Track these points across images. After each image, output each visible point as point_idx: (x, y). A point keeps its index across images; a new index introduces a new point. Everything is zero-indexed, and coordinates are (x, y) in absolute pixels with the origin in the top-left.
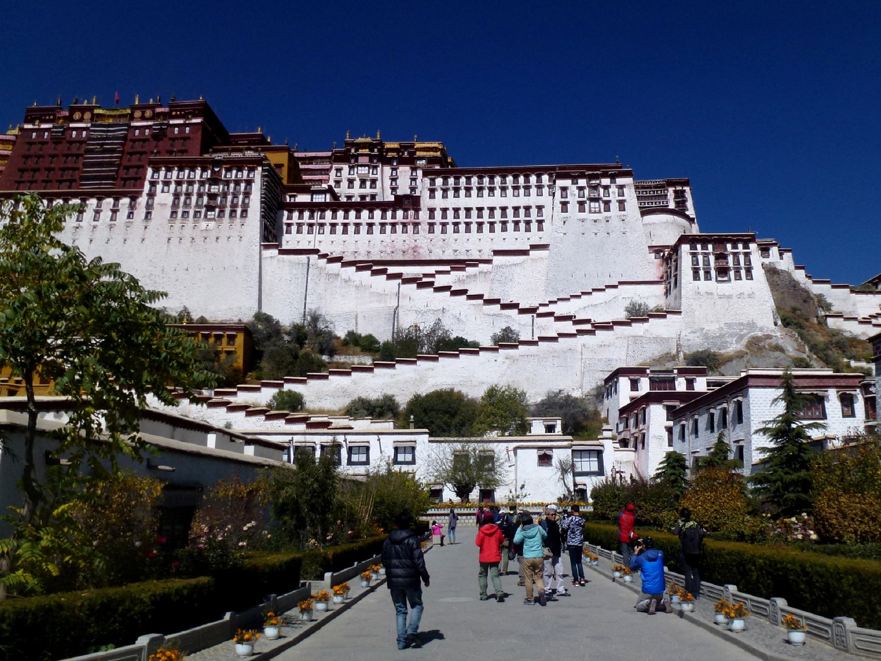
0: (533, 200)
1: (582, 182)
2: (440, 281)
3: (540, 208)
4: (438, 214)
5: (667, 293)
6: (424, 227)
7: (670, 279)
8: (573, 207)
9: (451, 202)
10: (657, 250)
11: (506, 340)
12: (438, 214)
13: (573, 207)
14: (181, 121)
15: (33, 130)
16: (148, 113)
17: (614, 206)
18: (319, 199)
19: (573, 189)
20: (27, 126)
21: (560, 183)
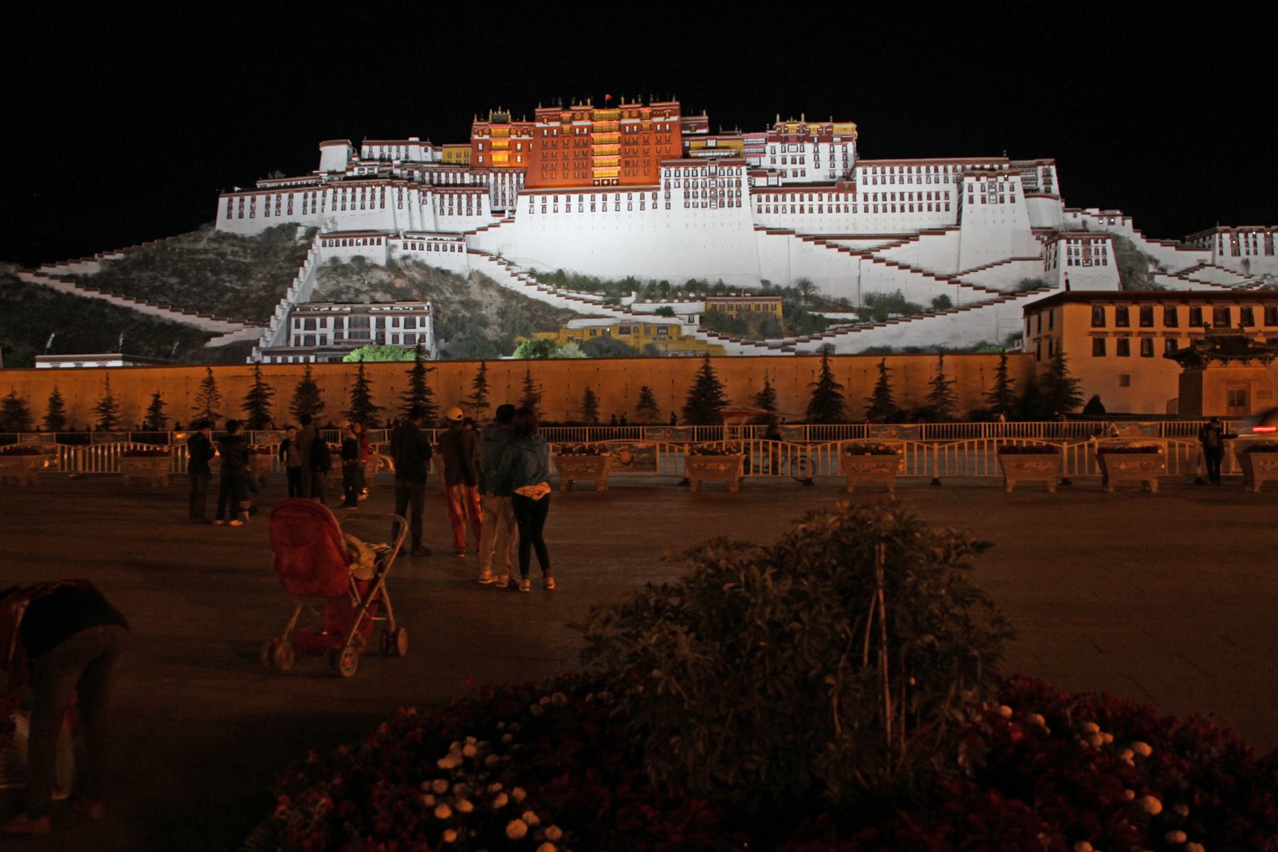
0: (942, 187)
1: (983, 179)
2: (883, 254)
3: (947, 195)
4: (870, 197)
5: (1047, 268)
6: (861, 208)
7: (1050, 262)
8: (977, 199)
9: (879, 188)
10: (1036, 231)
11: (942, 305)
12: (870, 197)
13: (977, 199)
14: (661, 119)
15: (542, 129)
16: (634, 113)
17: (1007, 199)
18: (773, 181)
19: (977, 186)
20: (539, 125)
21: (968, 180)
